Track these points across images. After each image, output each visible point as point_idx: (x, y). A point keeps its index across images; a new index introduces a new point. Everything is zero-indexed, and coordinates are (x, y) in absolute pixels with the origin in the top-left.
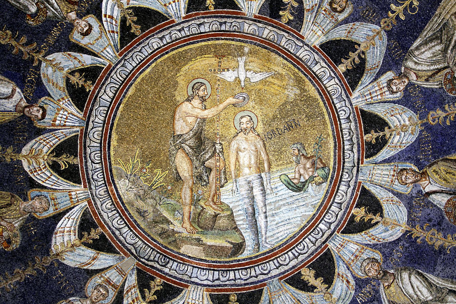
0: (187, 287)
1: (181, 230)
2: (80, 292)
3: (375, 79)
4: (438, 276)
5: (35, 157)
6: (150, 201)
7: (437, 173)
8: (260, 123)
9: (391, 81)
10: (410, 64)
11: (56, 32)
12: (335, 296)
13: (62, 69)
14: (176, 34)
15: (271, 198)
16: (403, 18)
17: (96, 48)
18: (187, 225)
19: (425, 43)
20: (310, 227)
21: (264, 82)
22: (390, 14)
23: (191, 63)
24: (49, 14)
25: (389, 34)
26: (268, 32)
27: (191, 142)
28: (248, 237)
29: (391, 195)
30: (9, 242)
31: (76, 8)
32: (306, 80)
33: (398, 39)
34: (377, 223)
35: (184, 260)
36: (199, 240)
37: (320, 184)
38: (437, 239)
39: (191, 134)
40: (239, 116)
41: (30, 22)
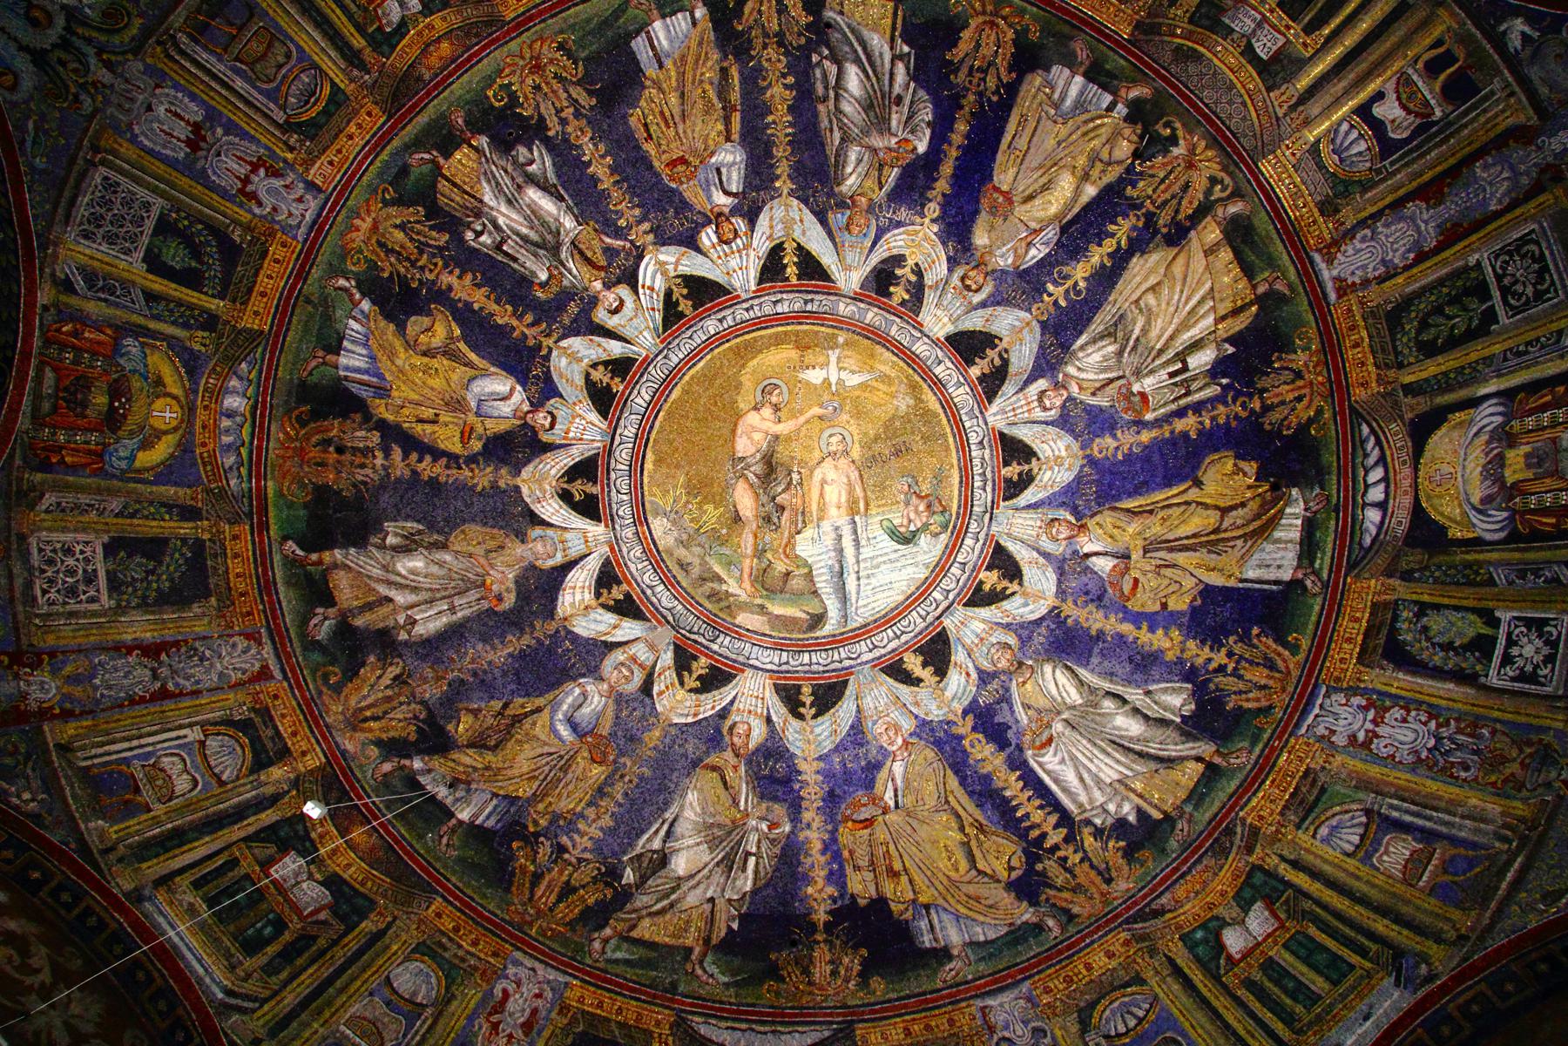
0: (743, 671)
1: (738, 591)
2: (594, 672)
3: (1021, 389)
4: (1092, 671)
5: (540, 482)
6: (697, 550)
7: (1101, 526)
8: (857, 445)
9: (1043, 392)
10: (1071, 370)
11: (573, 308)
12: (948, 694)
14: (741, 314)
15: (866, 552)
16: (1063, 303)
17: (628, 332)
18: (747, 584)
19: (1094, 341)
21: (863, 386)
22: (1045, 297)
23: (761, 356)
24: (565, 283)
25: (1044, 325)
26: (872, 316)
27: (758, 469)
29: (1035, 554)
30: (500, 598)
31: (603, 274)
32: (925, 386)
33: (1056, 334)
34: (1013, 594)
35: (738, 633)
36: (762, 607)
37: (937, 535)
38: (1096, 620)
39: (758, 456)
40: (826, 434)
41: (539, 294)
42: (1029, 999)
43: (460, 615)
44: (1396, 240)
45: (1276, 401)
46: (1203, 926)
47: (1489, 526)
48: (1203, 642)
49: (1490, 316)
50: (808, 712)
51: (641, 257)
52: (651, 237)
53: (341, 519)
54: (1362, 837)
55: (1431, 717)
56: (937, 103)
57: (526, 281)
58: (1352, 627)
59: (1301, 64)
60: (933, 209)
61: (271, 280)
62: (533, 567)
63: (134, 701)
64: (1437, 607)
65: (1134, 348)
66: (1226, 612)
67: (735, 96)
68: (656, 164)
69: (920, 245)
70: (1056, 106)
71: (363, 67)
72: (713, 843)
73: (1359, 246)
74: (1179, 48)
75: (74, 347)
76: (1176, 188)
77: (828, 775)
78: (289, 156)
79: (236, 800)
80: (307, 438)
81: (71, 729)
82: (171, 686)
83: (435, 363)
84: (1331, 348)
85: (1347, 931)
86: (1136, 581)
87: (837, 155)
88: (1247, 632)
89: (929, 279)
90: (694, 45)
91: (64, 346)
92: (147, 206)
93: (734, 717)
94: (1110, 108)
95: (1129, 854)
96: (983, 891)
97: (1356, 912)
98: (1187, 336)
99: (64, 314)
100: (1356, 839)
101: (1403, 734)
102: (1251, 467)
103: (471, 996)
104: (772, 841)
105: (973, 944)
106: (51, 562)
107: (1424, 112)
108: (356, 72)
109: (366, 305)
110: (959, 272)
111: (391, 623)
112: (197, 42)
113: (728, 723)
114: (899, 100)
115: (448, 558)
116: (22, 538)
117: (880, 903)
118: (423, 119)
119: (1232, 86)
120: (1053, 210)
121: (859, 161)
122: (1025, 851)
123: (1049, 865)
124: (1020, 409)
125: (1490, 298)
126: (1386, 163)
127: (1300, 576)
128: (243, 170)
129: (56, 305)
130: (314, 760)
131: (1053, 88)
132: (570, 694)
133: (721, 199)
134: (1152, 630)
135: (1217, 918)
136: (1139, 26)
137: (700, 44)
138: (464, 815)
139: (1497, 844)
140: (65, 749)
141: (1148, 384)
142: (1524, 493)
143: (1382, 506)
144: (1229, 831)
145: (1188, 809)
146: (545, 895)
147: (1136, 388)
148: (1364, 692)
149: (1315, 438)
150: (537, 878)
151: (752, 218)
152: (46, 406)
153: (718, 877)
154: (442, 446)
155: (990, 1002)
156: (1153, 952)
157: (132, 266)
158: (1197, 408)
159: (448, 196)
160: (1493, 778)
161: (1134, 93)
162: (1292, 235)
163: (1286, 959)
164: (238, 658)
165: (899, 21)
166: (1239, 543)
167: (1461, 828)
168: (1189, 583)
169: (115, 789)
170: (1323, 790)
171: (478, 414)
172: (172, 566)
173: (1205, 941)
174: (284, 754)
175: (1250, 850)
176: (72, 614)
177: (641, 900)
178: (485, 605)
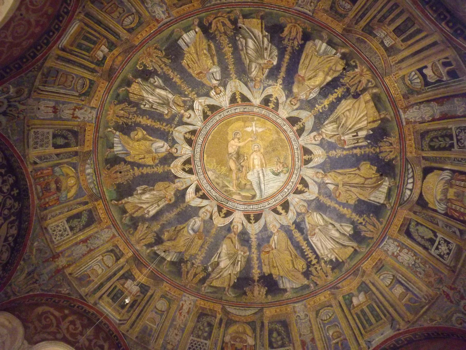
2: (197, 215)
5: (176, 167)
6: (221, 179)
10: (323, 130)
11: (177, 119)
12: (289, 218)
13: (181, 133)
15: (266, 178)
16: (321, 111)
17: (193, 123)
18: (235, 187)
19: (330, 123)
20: (280, 191)
25: (315, 117)
26: (264, 112)
27: (235, 156)
28: (258, 192)
30: (170, 200)
35: (234, 201)
36: (239, 193)
42: (305, 306)
43: (161, 206)
44: (427, 112)
45: (384, 150)
46: (348, 295)
47: (441, 208)
48: (357, 214)
49: (452, 146)
50: (252, 221)
51: (194, 101)
52: (196, 96)
53: (125, 191)
54: (391, 282)
55: (415, 255)
56: (279, 49)
57: (161, 115)
58: (398, 222)
59: (400, 51)
60: (280, 81)
61: (89, 136)
62: (177, 190)
63: (84, 255)
64: (422, 225)
65: (342, 127)
66: (364, 207)
67: (214, 52)
68: (193, 75)
69: (277, 92)
70: (317, 52)
71: (96, 72)
72: (230, 258)
73: (414, 110)
74: (358, 39)
75: (43, 177)
76: (357, 81)
77: (258, 239)
78: (83, 103)
79: (113, 271)
80: (111, 172)
81: (71, 268)
82: (92, 248)
83: (141, 143)
84: (402, 139)
85: (383, 308)
86: (340, 193)
87: (249, 66)
88: (369, 214)
89: (280, 101)
90: (198, 39)
91: (40, 178)
92: (48, 133)
93: (234, 224)
94: (335, 54)
95: (333, 269)
96: (296, 274)
97: (386, 303)
98: (358, 126)
99: (36, 170)
100: (389, 283)
101: (406, 257)
102: (375, 168)
103: (174, 307)
104: (244, 257)
105: (293, 288)
106: (54, 231)
107: (440, 76)
108: (95, 74)
109: (118, 133)
110: (289, 99)
111: (143, 213)
112: (45, 86)
113: (232, 225)
114: (266, 49)
115: (155, 192)
116: (46, 228)
117: (270, 275)
118: (119, 80)
119: (376, 53)
120: (317, 83)
121: (256, 67)
122: (307, 264)
123: (312, 269)
124: (307, 140)
125: (453, 140)
126: (426, 88)
127: (385, 203)
128: (71, 112)
129: (34, 169)
130: (131, 254)
131: (316, 46)
132: (192, 222)
133: (215, 82)
134: (344, 208)
135: (351, 293)
136: (344, 29)
137: (200, 38)
138: (169, 259)
139: (423, 300)
140: (70, 274)
141: (346, 137)
142: (452, 203)
143: (411, 190)
144: (358, 270)
145: (348, 260)
146: (190, 276)
147: (342, 138)
148: (398, 241)
149: (394, 165)
150: (188, 272)
151: (225, 86)
152: (41, 194)
153: (231, 268)
154: (148, 164)
155: (296, 305)
156: (335, 298)
157: (50, 150)
158: (360, 147)
159: (133, 98)
160: (426, 280)
161: (343, 51)
162: (393, 103)
163: (367, 311)
164: (106, 235)
165: (263, 26)
166: (369, 189)
167: (415, 290)
168: (354, 197)
169: (84, 279)
170: (383, 266)
171: (156, 153)
172: (84, 218)
173: (348, 299)
174: (123, 253)
175: (362, 276)
176: (63, 241)
177: (213, 275)
178: (167, 202)
